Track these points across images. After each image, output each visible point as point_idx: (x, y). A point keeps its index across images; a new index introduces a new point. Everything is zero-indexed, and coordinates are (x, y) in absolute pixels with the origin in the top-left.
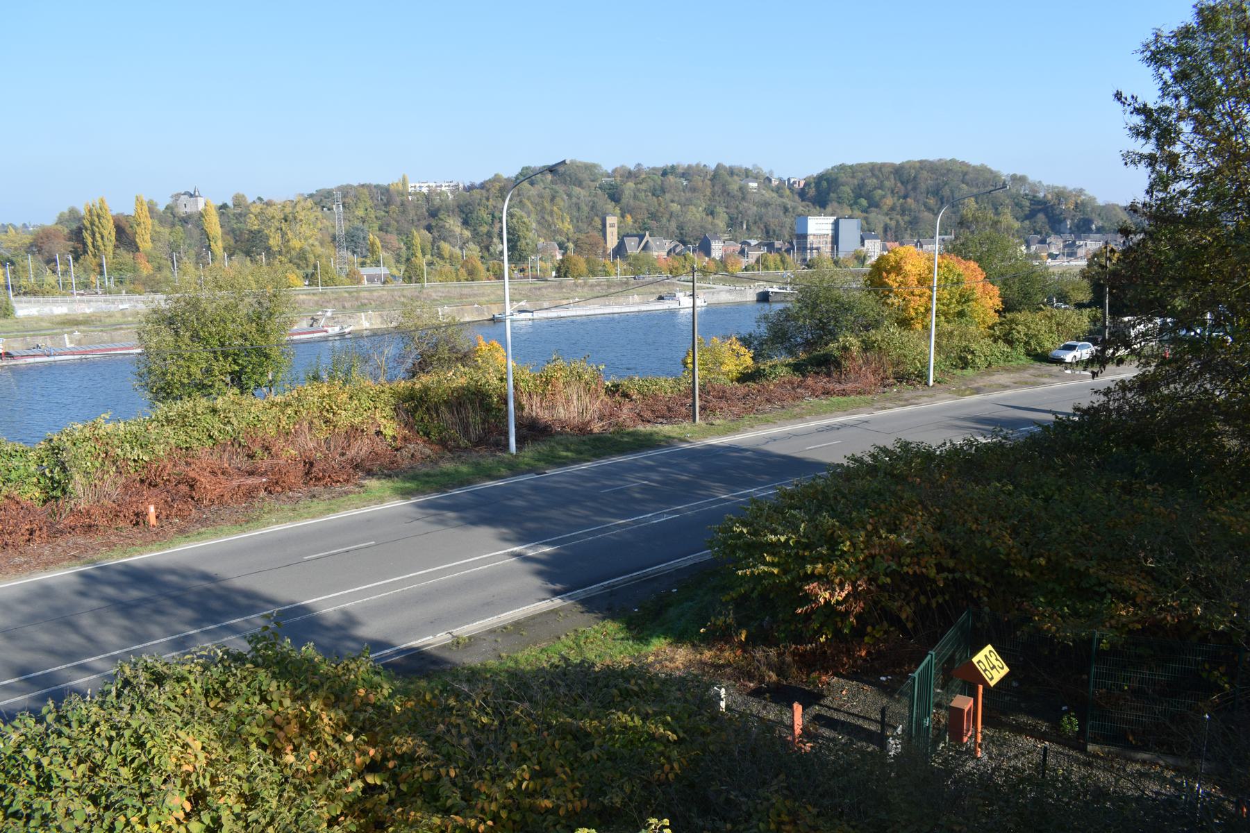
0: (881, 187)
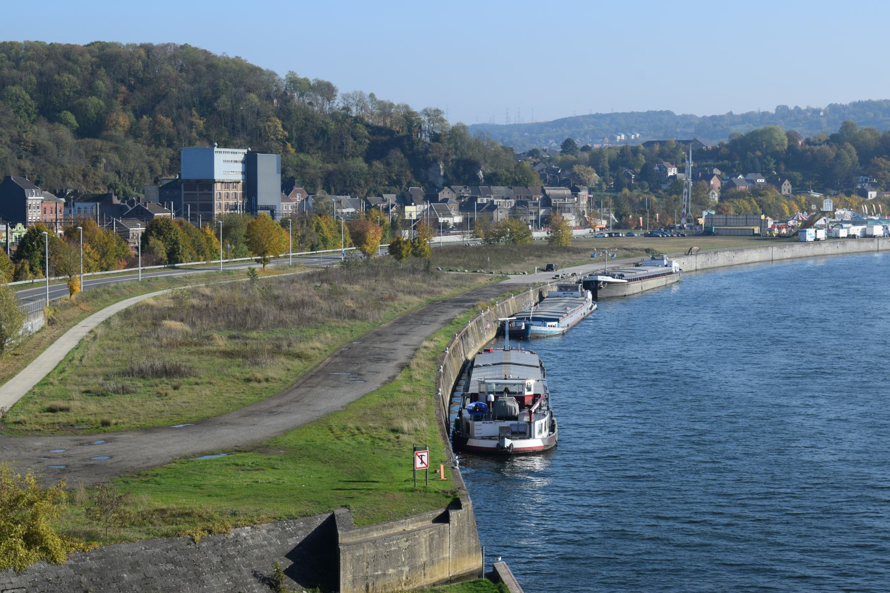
0: (91, 89)
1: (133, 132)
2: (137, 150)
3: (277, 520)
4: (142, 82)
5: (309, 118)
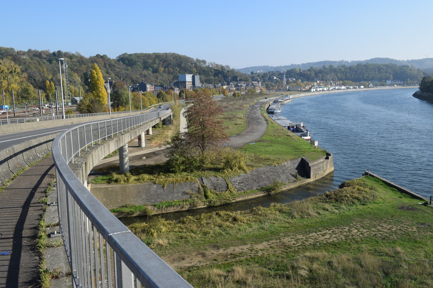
0: (154, 63)
1: (164, 72)
2: (165, 75)
3: (291, 160)
4: (165, 61)
5: (201, 68)
